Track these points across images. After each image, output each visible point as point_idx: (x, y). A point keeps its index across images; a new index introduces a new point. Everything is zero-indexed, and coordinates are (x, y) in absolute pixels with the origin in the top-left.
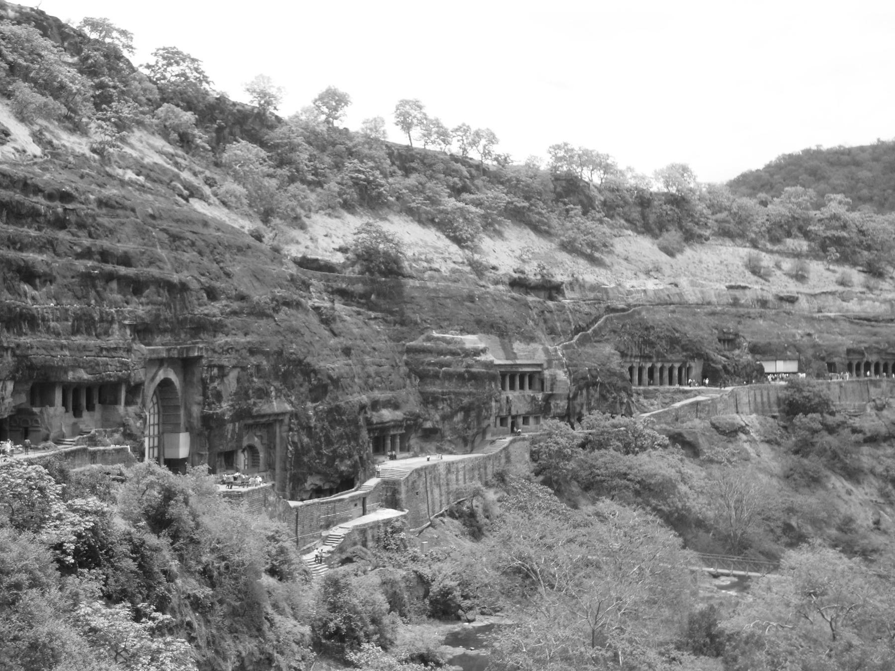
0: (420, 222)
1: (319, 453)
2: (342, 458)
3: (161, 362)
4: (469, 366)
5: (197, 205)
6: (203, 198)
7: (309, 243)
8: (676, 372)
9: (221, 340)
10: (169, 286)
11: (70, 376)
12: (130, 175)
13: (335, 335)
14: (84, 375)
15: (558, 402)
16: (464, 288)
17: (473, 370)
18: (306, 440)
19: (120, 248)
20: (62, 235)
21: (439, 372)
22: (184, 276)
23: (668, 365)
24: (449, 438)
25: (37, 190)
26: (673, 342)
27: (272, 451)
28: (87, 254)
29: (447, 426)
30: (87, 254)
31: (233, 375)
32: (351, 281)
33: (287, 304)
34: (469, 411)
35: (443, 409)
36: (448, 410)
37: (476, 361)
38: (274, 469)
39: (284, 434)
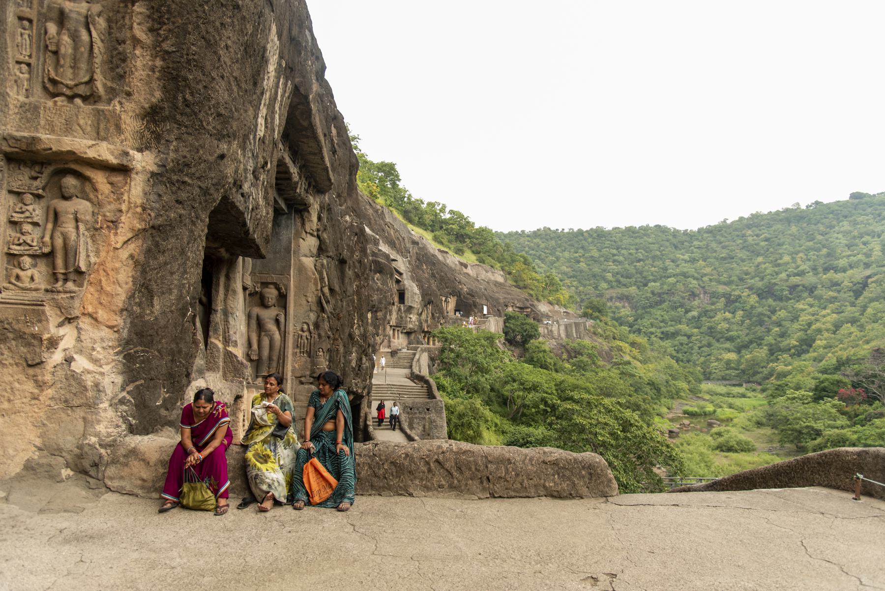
27: (268, 315)
34: (376, 311)
37: (380, 250)
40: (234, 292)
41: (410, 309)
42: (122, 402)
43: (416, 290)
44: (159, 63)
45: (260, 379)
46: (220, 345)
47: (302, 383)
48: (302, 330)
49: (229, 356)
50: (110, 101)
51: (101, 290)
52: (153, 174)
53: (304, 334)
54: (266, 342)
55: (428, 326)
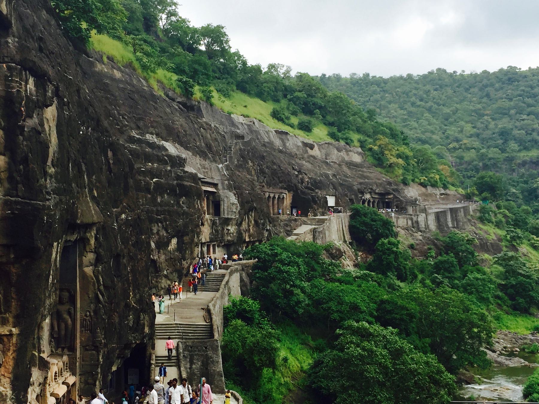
1: (127, 305)
4: (178, 178)
8: (276, 202)
15: (229, 228)
17: (186, 183)
21: (148, 184)
23: (272, 195)
24: (165, 272)
26: (274, 173)
27: (63, 308)
29: (163, 257)
34: (182, 236)
35: (158, 233)
36: (164, 233)
38: (72, 349)
39: (89, 270)
40: (42, 328)
41: (227, 221)
42: (13, 398)
43: (233, 199)
44: (19, 303)
45: (60, 349)
46: (37, 354)
47: (87, 350)
48: (86, 316)
49: (41, 359)
50: (5, 314)
51: (6, 368)
52: (18, 334)
53: (88, 318)
54: (63, 326)
55: (249, 236)
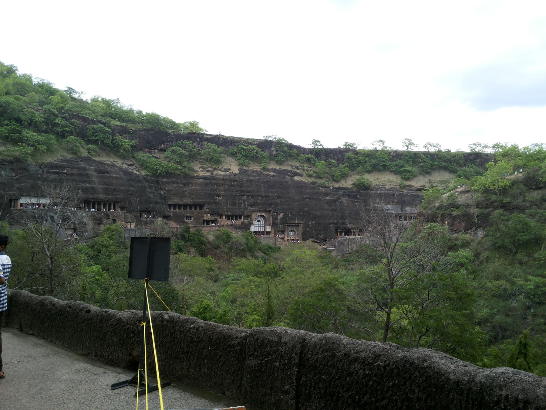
0: (395, 174)
2: (321, 235)
3: (260, 211)
5: (296, 178)
6: (300, 175)
7: (344, 183)
9: (279, 207)
10: (262, 196)
11: (225, 213)
12: (272, 173)
13: (330, 205)
14: (230, 214)
16: (392, 192)
18: (308, 229)
19: (249, 189)
20: (232, 188)
22: (271, 194)
25: (226, 180)
28: (237, 191)
30: (237, 191)
31: (282, 215)
32: (352, 192)
33: (309, 199)
